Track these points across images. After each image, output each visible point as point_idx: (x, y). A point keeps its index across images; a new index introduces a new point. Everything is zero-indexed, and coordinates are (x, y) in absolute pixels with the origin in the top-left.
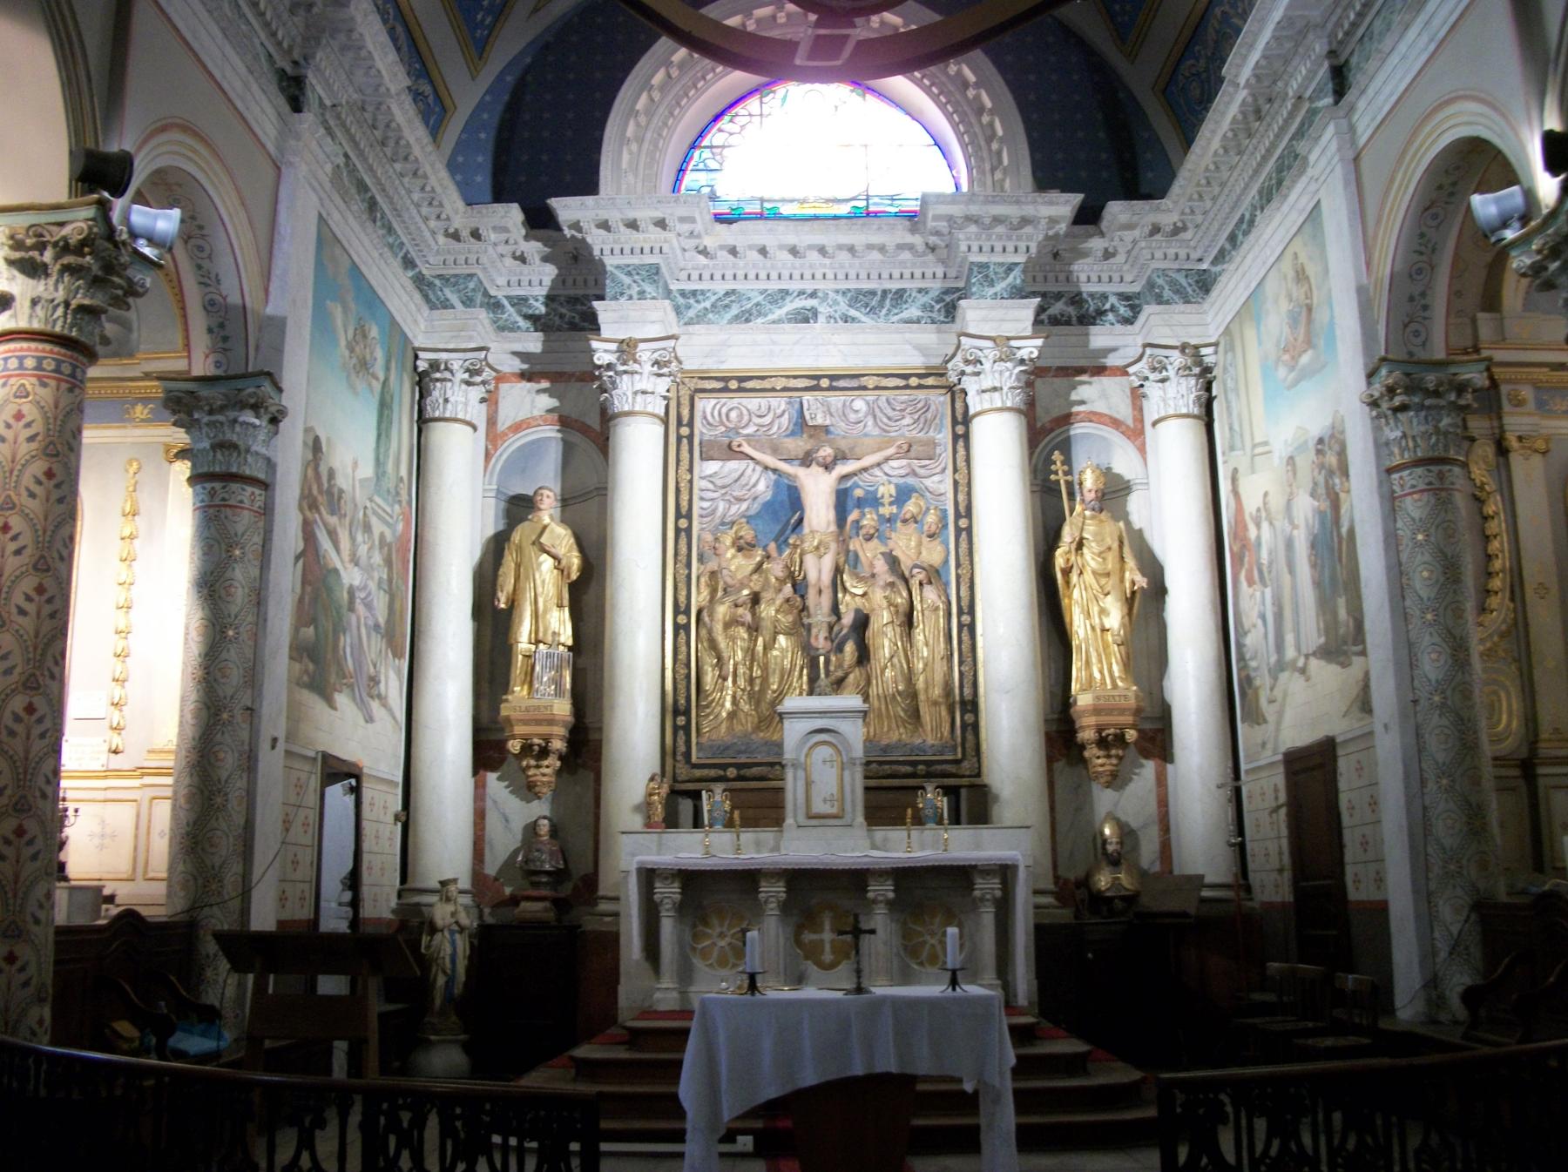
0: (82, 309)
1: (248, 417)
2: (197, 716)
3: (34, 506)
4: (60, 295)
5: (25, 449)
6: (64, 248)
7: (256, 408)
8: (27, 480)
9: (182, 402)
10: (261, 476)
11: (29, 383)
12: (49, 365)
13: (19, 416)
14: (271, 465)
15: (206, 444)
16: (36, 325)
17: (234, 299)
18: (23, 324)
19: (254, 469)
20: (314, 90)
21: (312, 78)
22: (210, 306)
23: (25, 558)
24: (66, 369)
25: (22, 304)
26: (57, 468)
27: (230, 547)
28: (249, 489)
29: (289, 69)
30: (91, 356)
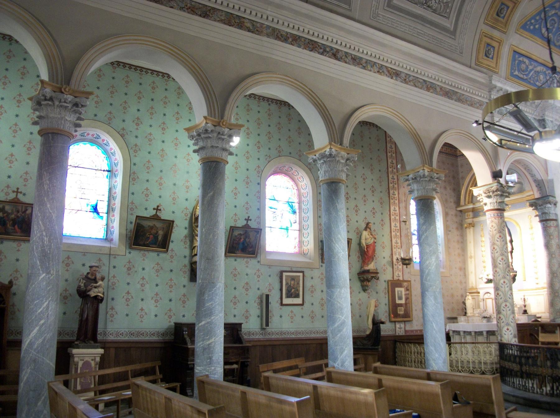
0: (500, 202)
1: (549, 205)
2: (549, 275)
3: (498, 243)
4: (495, 201)
5: (495, 232)
6: (493, 192)
7: (550, 203)
8: (496, 238)
9: (534, 204)
10: (555, 218)
11: (493, 219)
12: (496, 215)
13: (492, 226)
14: (556, 215)
15: (540, 214)
16: (492, 208)
17: (540, 178)
18: (490, 208)
19: (552, 217)
20: (548, 120)
21: (546, 118)
22: (535, 181)
23: (498, 254)
24: (499, 215)
25: (488, 204)
26: (501, 235)
27: (550, 236)
28: (552, 222)
29: (541, 118)
30: (504, 210)
